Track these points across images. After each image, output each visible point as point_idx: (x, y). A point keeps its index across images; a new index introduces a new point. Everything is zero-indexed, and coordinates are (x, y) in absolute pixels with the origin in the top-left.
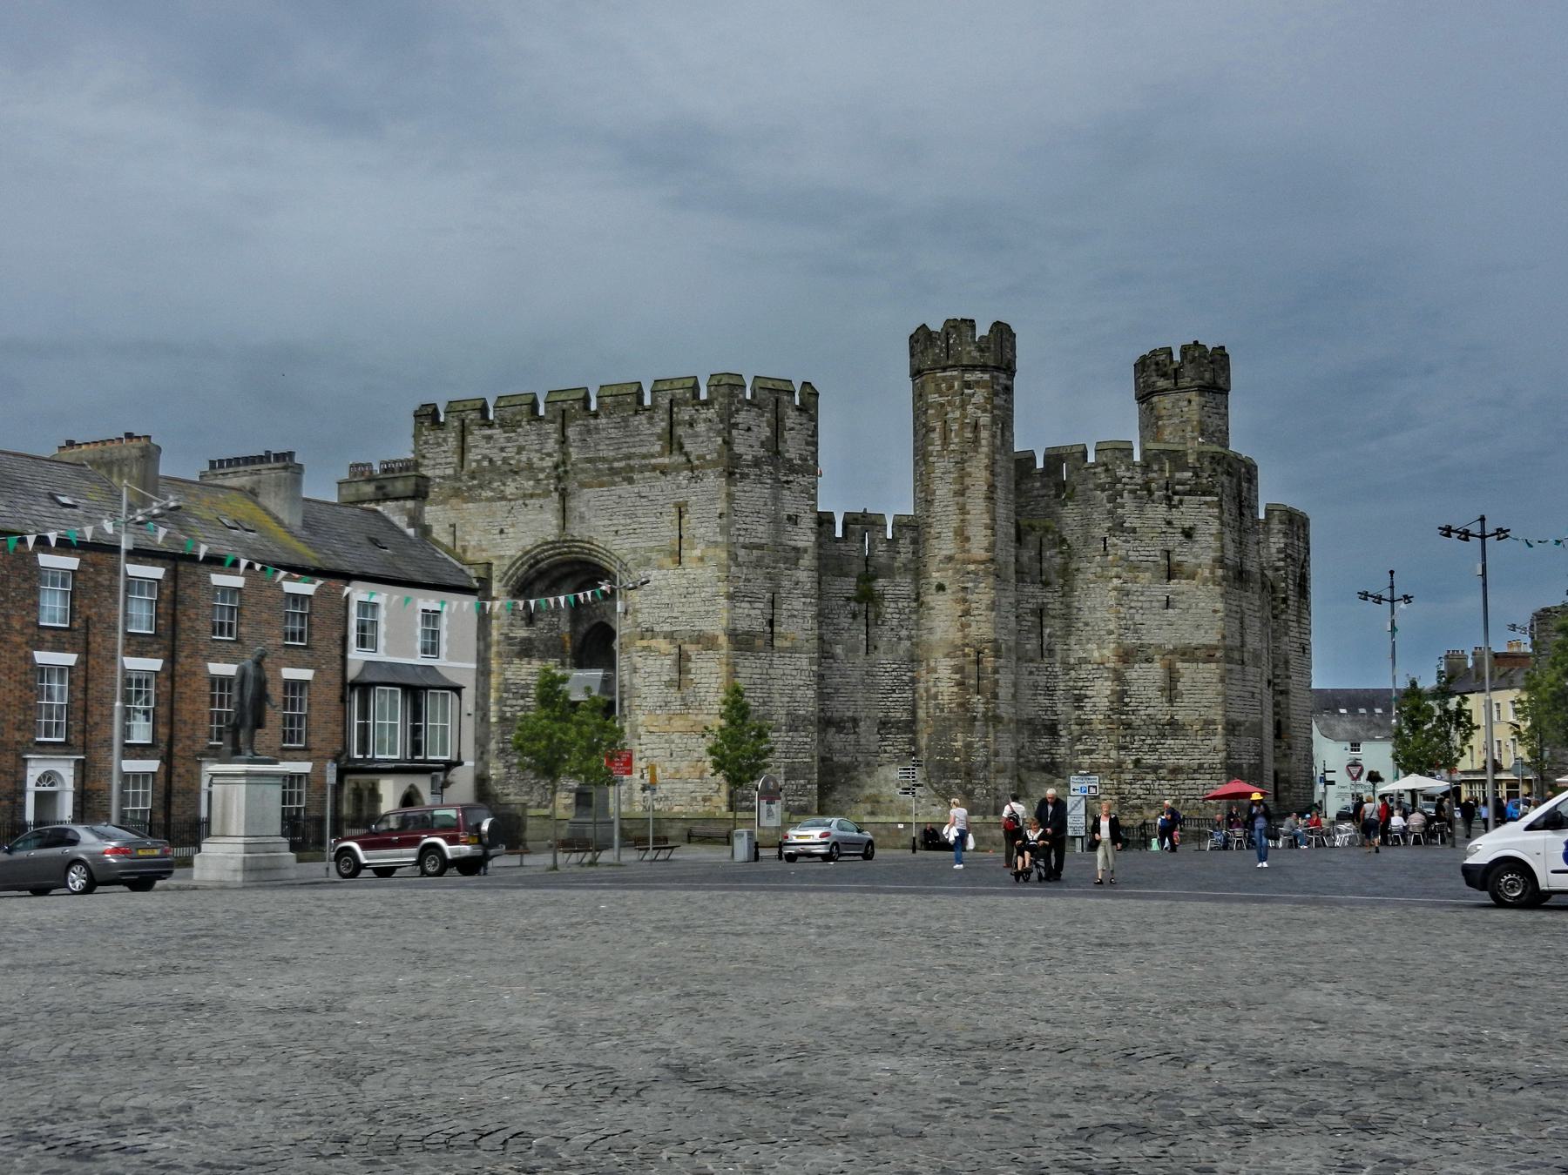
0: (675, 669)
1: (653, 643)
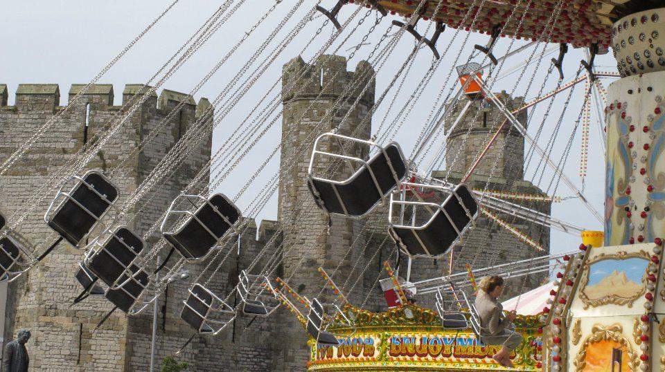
1: (57, 319)
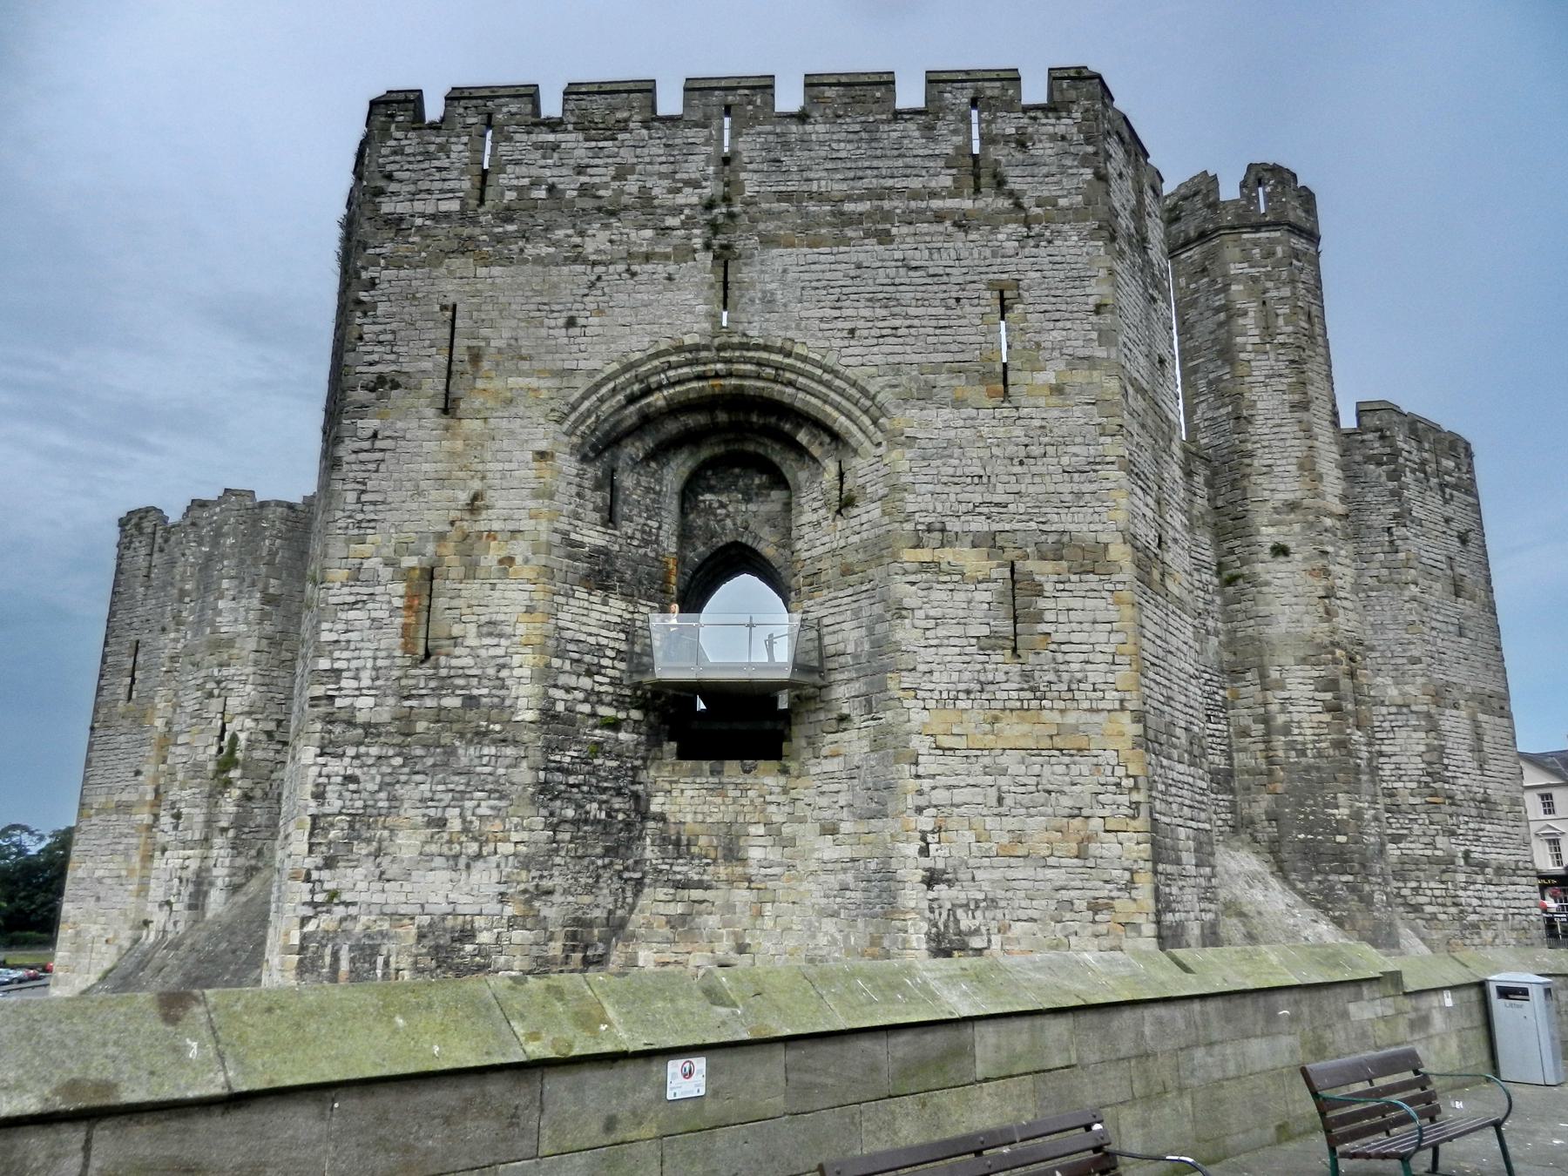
0: (1004, 611)
1: (947, 555)
